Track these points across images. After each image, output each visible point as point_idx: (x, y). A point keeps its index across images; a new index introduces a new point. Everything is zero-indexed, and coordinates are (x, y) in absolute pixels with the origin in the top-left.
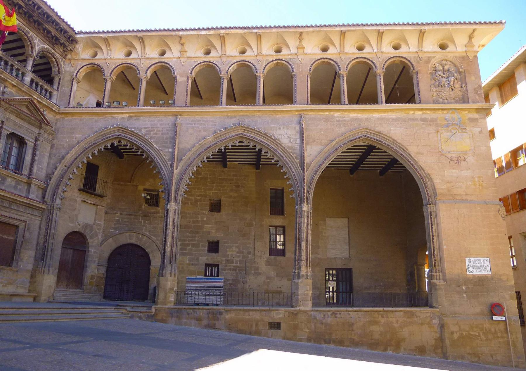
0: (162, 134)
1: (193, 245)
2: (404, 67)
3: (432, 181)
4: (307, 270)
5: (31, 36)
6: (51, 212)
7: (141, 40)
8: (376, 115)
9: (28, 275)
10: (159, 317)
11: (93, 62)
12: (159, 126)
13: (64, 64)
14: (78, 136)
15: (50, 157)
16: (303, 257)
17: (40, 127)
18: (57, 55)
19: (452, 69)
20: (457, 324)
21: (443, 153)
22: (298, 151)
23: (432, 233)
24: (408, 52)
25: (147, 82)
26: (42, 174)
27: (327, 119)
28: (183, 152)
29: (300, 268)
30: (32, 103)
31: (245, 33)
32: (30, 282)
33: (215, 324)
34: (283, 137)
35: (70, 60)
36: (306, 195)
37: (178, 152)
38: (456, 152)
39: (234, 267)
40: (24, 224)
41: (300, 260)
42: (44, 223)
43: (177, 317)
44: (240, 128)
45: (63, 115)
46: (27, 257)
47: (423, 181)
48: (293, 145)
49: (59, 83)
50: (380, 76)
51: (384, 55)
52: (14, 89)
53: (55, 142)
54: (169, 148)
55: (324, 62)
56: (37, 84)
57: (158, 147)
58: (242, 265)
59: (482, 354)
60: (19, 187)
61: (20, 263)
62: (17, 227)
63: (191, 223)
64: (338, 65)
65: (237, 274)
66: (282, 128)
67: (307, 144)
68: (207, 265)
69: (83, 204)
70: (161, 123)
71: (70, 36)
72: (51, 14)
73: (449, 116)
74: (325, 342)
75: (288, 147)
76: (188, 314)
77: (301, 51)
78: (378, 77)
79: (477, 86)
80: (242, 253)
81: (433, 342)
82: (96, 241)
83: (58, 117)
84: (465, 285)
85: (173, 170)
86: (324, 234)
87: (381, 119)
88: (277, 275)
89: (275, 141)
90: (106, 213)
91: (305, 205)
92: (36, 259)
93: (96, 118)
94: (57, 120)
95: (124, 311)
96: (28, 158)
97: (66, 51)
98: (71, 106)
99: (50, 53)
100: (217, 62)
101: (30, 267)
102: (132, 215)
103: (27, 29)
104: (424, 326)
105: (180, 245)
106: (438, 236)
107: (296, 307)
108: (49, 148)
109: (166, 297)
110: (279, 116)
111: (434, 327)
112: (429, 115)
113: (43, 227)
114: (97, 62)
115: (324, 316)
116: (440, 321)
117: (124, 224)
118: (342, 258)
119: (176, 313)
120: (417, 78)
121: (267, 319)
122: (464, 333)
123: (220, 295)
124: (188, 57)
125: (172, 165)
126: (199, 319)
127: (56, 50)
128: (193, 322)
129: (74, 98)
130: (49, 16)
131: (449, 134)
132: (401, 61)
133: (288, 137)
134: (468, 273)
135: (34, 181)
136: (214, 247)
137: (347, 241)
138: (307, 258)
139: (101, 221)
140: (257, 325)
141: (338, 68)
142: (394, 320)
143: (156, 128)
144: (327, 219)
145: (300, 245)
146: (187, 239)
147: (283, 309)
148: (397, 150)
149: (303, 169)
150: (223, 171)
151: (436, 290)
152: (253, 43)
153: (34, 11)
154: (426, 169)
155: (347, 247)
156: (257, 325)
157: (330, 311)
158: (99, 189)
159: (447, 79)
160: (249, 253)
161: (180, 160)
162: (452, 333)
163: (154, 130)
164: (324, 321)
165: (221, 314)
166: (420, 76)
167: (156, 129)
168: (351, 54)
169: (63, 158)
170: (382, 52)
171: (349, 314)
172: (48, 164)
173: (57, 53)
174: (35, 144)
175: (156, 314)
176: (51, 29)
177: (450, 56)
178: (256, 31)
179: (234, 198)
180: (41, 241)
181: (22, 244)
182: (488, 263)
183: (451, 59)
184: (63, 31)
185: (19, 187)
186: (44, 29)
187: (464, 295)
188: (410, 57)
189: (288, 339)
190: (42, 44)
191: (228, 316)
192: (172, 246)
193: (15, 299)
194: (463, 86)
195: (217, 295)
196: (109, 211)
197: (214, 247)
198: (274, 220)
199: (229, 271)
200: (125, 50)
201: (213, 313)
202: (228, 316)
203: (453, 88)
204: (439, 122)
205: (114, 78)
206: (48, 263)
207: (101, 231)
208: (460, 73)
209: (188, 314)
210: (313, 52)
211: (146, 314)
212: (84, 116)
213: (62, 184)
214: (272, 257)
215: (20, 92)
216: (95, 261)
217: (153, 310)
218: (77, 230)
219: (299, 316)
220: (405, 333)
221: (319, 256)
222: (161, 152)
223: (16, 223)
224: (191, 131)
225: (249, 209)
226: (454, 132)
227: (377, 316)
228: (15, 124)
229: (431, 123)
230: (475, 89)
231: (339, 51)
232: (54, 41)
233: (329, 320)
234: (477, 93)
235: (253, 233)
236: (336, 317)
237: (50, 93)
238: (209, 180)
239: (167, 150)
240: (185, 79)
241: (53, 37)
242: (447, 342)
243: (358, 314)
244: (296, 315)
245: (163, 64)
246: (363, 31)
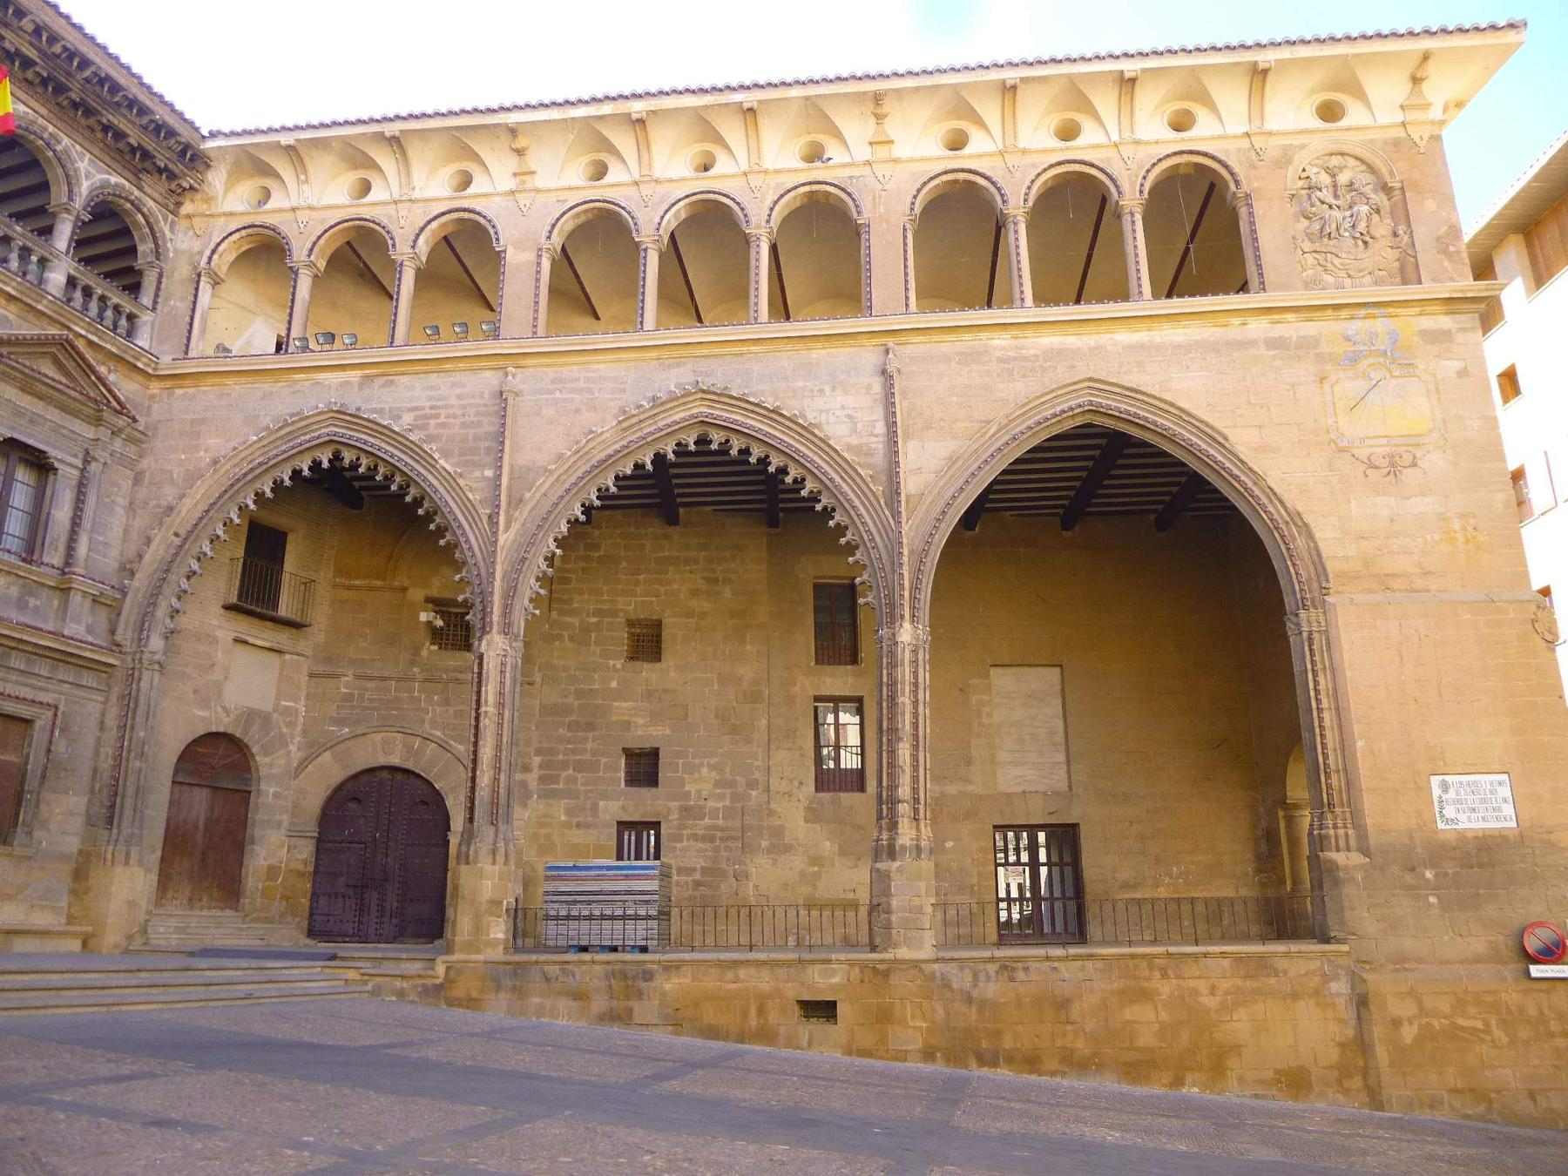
0: (463, 425)
1: (580, 766)
2: (1212, 186)
3: (1310, 536)
4: (918, 830)
5: (66, 151)
6: (132, 677)
7: (395, 142)
8: (1123, 337)
9: (66, 870)
10: (459, 991)
11: (258, 220)
12: (454, 401)
13: (172, 230)
14: (214, 444)
15: (131, 508)
16: (904, 791)
17: (98, 421)
18: (151, 203)
19: (1364, 179)
20: (1411, 993)
21: (1344, 444)
22: (879, 458)
23: (1318, 701)
24: (1219, 137)
25: (418, 270)
26: (109, 562)
27: (968, 357)
28: (523, 477)
29: (893, 826)
30: (66, 346)
31: (707, 107)
32: (73, 892)
33: (630, 1012)
34: (832, 418)
35: (189, 217)
36: (907, 594)
37: (511, 479)
38: (1384, 441)
39: (708, 828)
40: (50, 714)
41: (894, 802)
42: (113, 712)
43: (514, 989)
44: (700, 395)
45: (169, 384)
46: (62, 816)
47: (1282, 537)
48: (865, 440)
49: (158, 289)
50: (1132, 215)
51: (1142, 148)
52: (13, 307)
53: (144, 464)
54: (482, 466)
55: (956, 181)
56: (88, 292)
57: (452, 465)
58: (729, 823)
59: (1498, 1092)
60: (32, 602)
61: (37, 834)
62: (28, 722)
63: (570, 700)
64: (999, 189)
65: (716, 850)
66: (827, 389)
67: (907, 437)
68: (623, 826)
69: (240, 648)
70: (458, 391)
71: (187, 147)
72: (122, 81)
73: (1356, 327)
74: (982, 1061)
75: (849, 447)
76: (548, 980)
77: (882, 152)
78: (1127, 217)
79: (1442, 231)
80: (732, 784)
81: (1334, 1055)
82: (282, 762)
83: (155, 387)
84: (1432, 866)
85: (495, 533)
86: (985, 720)
87: (1141, 347)
88: (842, 852)
89: (806, 431)
90: (311, 676)
91: (907, 625)
92: (90, 822)
93: (266, 386)
94: (152, 397)
95: (352, 975)
96: (61, 515)
97: (177, 195)
98: (191, 355)
99: (127, 199)
100: (627, 198)
101: (72, 844)
102: (390, 678)
103: (51, 128)
104: (1301, 1003)
105: (540, 767)
106: (1337, 709)
107: (885, 950)
108: (126, 484)
109: (478, 928)
110: (818, 353)
111: (1334, 1005)
112: (1293, 328)
113: (112, 722)
114: (269, 220)
115: (975, 976)
116: (1352, 989)
117: (366, 708)
118: (1045, 794)
119: (510, 977)
120: (1251, 214)
121: (794, 991)
122: (1436, 1023)
123: (648, 917)
124: (538, 191)
125: (493, 519)
126: (580, 996)
127: (147, 189)
128: (563, 1004)
129: (203, 330)
130: (115, 88)
131: (1362, 385)
132: (1196, 164)
133: (849, 417)
134: (1441, 826)
135: (79, 583)
136: (644, 767)
137: (1060, 737)
138: (915, 790)
139: (296, 700)
140: (761, 1011)
141: (998, 198)
142: (1202, 986)
143: (445, 407)
144: (993, 671)
145: (892, 752)
146: (561, 747)
147: (842, 957)
148: (1195, 440)
149: (896, 514)
150: (666, 536)
151: (1336, 883)
152: (733, 132)
153: (69, 74)
154: (1294, 500)
155: (1061, 757)
156: (761, 1011)
157: (992, 960)
158: (286, 606)
159: (1348, 213)
160: (753, 784)
161: (516, 502)
162: (1396, 1023)
163: (437, 416)
164: (975, 993)
165: (648, 976)
166: (1259, 208)
167: (443, 413)
168: (1037, 152)
169: (170, 509)
170: (1137, 142)
171: (1055, 969)
172: (126, 530)
173: (148, 198)
174: (83, 470)
175: (449, 981)
177: (1352, 142)
178: (738, 97)
179: (703, 615)
180: (106, 765)
181: (43, 777)
182: (1505, 792)
183: (1357, 151)
184: (161, 130)
185: (32, 602)
186: (106, 128)
187: (1432, 899)
188: (1227, 152)
189: (862, 1053)
190: (100, 172)
191: (671, 985)
192: (498, 770)
193: (21, 945)
194: (1401, 230)
195: (636, 918)
196: (320, 669)
197: (644, 767)
198: (828, 680)
199: (692, 843)
200: (350, 178)
201: (624, 976)
202: (671, 985)
203: (1367, 238)
204: (1325, 348)
205: (322, 264)
206: (126, 831)
207: (299, 728)
208: (1386, 189)
209: (548, 980)
210: (917, 154)
211: (420, 981)
212: (229, 381)
213: (167, 590)
214: (825, 796)
215: (30, 317)
216: (280, 824)
217: (441, 969)
218: (221, 730)
219: (894, 980)
220: (1240, 1025)
221: (970, 788)
222: (461, 482)
223: (24, 711)
224: (548, 412)
225: (748, 647)
226: (1376, 376)
227: (1146, 973)
228: (18, 412)
230: (1438, 238)
231: (1001, 147)
232: (137, 160)
233: (991, 989)
234: (1444, 251)
235: (764, 722)
236: (1012, 979)
237: (131, 318)
238: (624, 564)
239: (477, 474)
240: (532, 256)
241: (133, 150)
242: (1382, 1055)
243: (1083, 968)
244: (886, 974)
245: (466, 215)
246: (1070, 78)
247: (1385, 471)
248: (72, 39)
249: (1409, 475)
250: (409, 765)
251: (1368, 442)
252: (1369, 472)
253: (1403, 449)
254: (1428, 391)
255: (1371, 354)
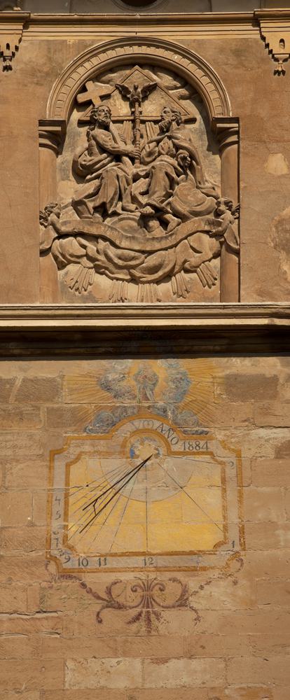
131: (117, 465)
204: (66, 400)
229: (26, 408)
247: (134, 612)
249: (174, 622)
251: (112, 563)
252: (107, 614)
253: (168, 575)
254: (224, 480)
255: (139, 413)
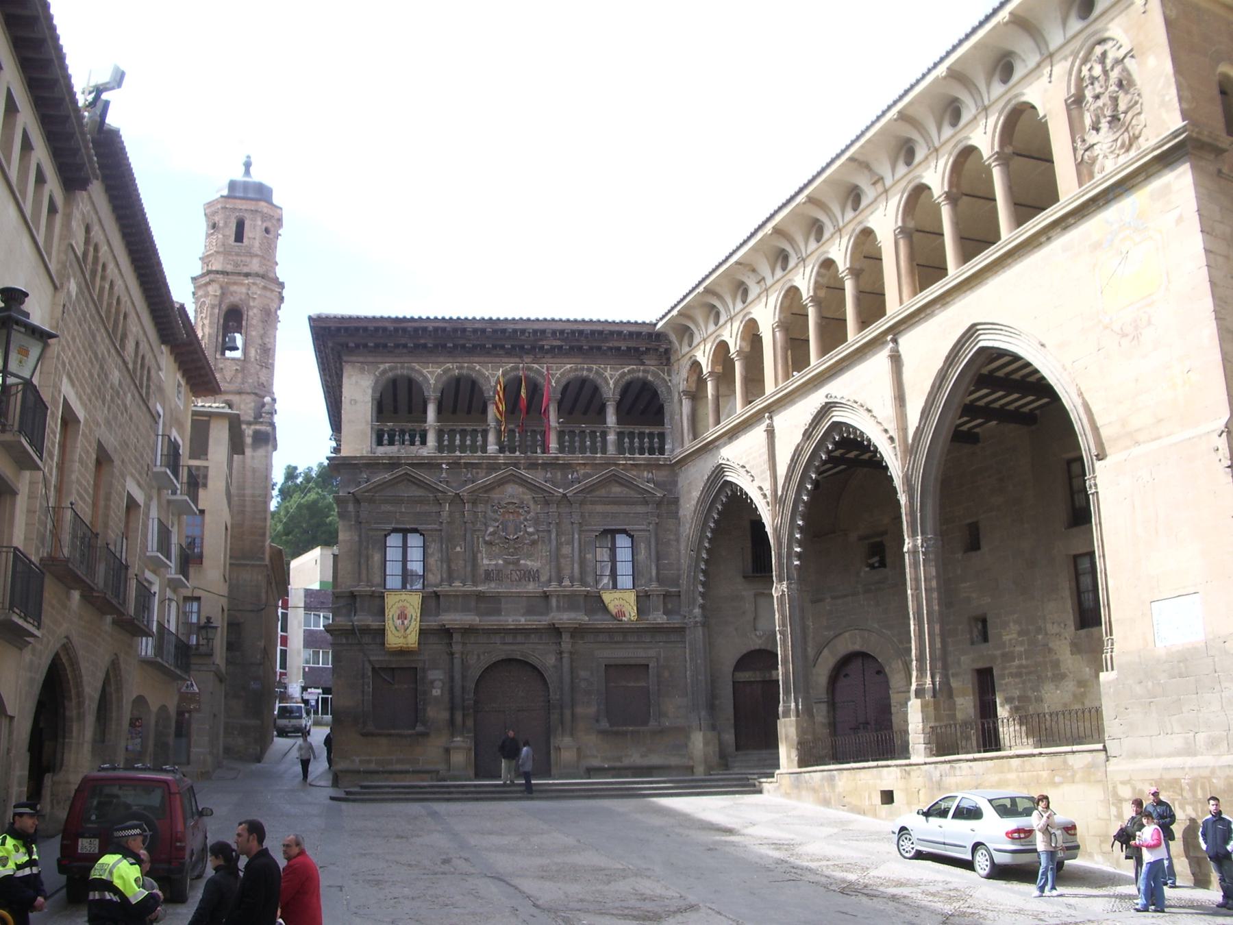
13: (669, 375)
46: (674, 708)
130: (601, 333)
176: (616, 344)
186: (611, 349)
214: (1083, 632)
218: (757, 647)
248: (569, 327)
250: (864, 649)
